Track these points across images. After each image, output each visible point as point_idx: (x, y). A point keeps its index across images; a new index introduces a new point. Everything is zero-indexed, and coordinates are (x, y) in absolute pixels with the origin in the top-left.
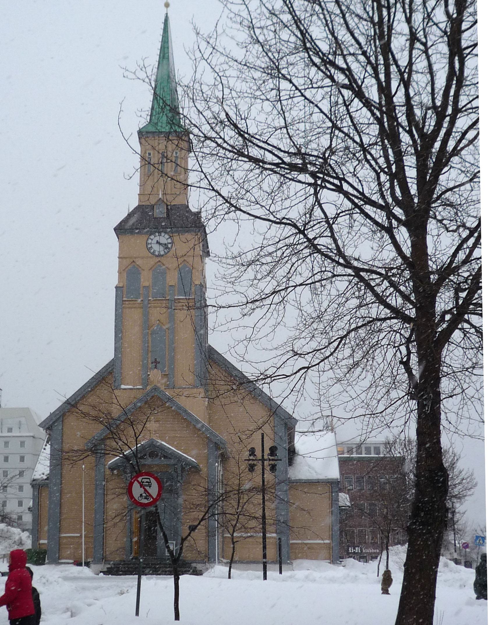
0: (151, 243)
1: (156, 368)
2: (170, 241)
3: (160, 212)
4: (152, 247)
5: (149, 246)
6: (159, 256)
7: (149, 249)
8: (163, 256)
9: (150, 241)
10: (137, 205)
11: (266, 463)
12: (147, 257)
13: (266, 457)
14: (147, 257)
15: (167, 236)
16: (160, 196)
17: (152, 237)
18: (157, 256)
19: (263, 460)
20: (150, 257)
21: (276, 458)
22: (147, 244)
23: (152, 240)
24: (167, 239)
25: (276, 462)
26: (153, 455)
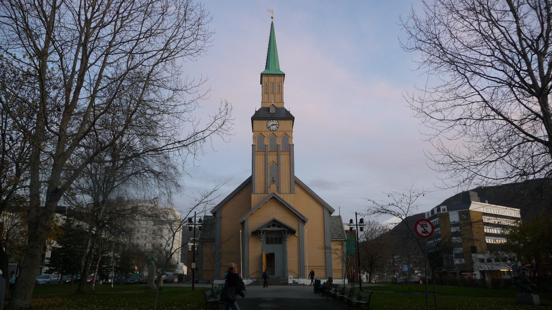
3: (272, 111)
6: (273, 131)
7: (268, 128)
8: (274, 131)
9: (268, 124)
10: (261, 107)
11: (358, 226)
12: (267, 131)
13: (358, 224)
14: (267, 131)
15: (276, 122)
17: (269, 122)
19: (357, 225)
20: (269, 131)
21: (353, 224)
22: (267, 125)
25: (363, 226)
26: (274, 225)
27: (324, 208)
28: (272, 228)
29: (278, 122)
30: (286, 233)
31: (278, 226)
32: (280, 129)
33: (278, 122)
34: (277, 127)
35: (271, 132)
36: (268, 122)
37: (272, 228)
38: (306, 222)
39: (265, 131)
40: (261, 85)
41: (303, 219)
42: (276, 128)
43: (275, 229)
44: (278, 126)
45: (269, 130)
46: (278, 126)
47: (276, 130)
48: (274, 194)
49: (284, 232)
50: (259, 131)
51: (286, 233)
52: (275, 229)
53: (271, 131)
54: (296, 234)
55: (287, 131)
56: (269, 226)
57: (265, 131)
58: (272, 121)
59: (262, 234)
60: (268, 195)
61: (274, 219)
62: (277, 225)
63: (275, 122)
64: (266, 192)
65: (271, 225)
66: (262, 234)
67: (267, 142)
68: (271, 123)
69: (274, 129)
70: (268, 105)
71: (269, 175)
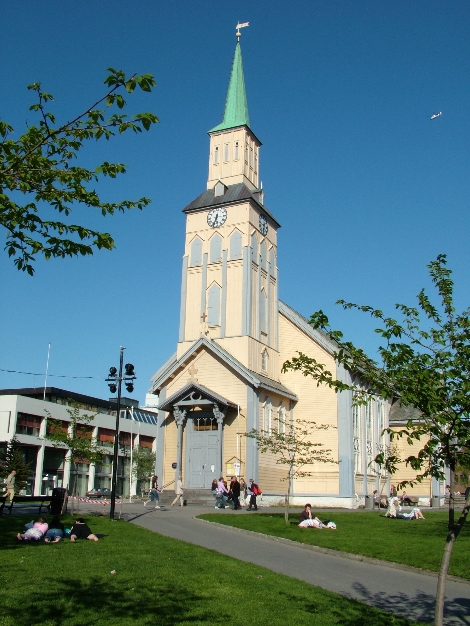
0: (211, 218)
4: (211, 221)
5: (209, 221)
9: (210, 216)
12: (207, 230)
14: (207, 230)
15: (223, 210)
17: (212, 213)
22: (208, 219)
23: (211, 215)
24: (223, 213)
26: (196, 397)
32: (227, 223)
33: (226, 211)
34: (223, 220)
35: (214, 230)
42: (222, 222)
44: (225, 218)
46: (225, 218)
49: (212, 406)
55: (239, 224)
56: (189, 399)
57: (203, 231)
58: (215, 210)
61: (192, 385)
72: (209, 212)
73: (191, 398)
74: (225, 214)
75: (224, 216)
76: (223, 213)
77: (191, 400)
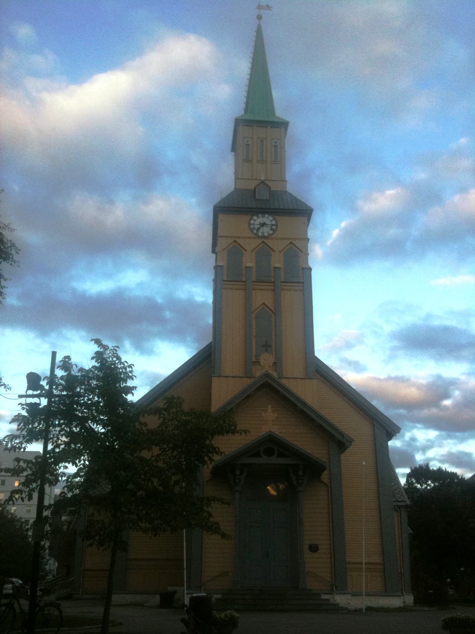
0: (254, 224)
1: (266, 351)
2: (274, 223)
5: (252, 227)
6: (263, 237)
7: (251, 230)
9: (252, 222)
12: (249, 238)
14: (249, 238)
16: (263, 179)
17: (255, 218)
18: (260, 237)
22: (250, 224)
23: (255, 220)
24: (271, 221)
26: (269, 452)
27: (375, 423)
28: (264, 460)
29: (275, 219)
30: (301, 473)
31: (280, 455)
34: (272, 229)
35: (260, 241)
36: (251, 219)
37: (264, 460)
38: (348, 447)
39: (244, 238)
40: (233, 153)
41: (340, 438)
42: (271, 232)
43: (274, 460)
44: (274, 227)
45: (256, 234)
47: (270, 235)
48: (267, 375)
50: (230, 237)
51: (301, 473)
52: (274, 460)
53: (260, 237)
54: (325, 476)
56: (257, 455)
57: (244, 238)
58: (260, 215)
59: (238, 472)
60: (252, 380)
62: (276, 452)
63: (268, 219)
64: (248, 374)
65: (262, 452)
66: (238, 472)
67: (249, 261)
68: (258, 220)
69: (266, 234)
70: (251, 185)
71: (254, 334)
72: (251, 216)
73: (262, 454)
74: (274, 223)
75: (272, 225)
76: (271, 221)
77: (261, 456)
